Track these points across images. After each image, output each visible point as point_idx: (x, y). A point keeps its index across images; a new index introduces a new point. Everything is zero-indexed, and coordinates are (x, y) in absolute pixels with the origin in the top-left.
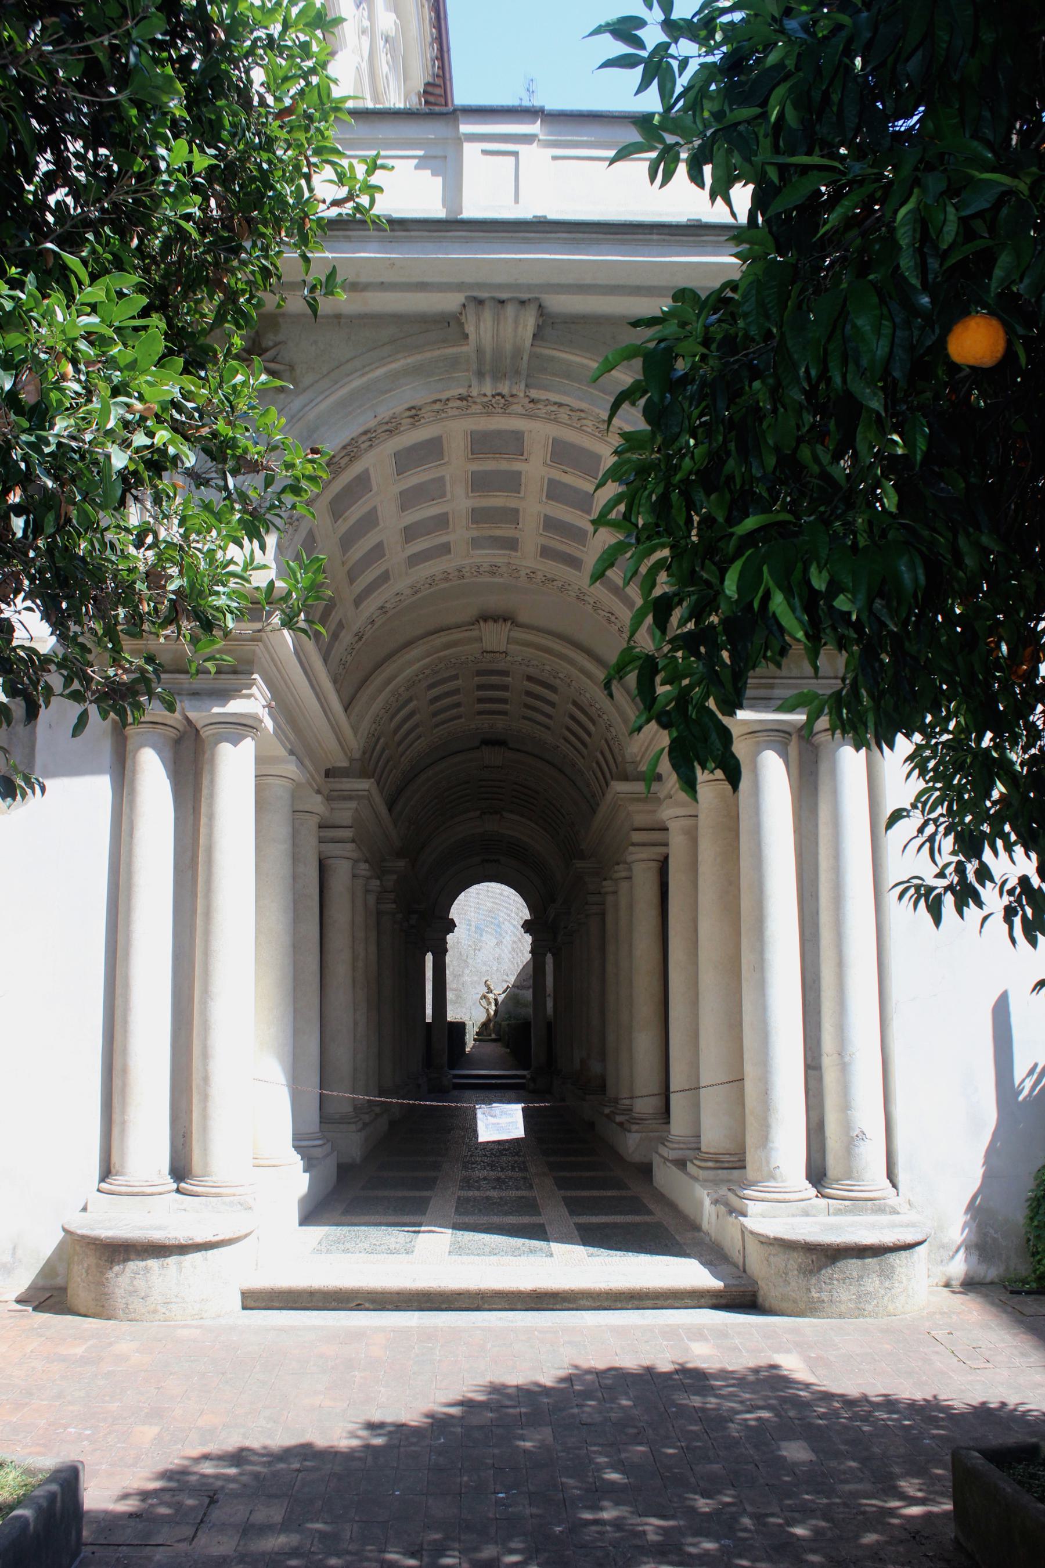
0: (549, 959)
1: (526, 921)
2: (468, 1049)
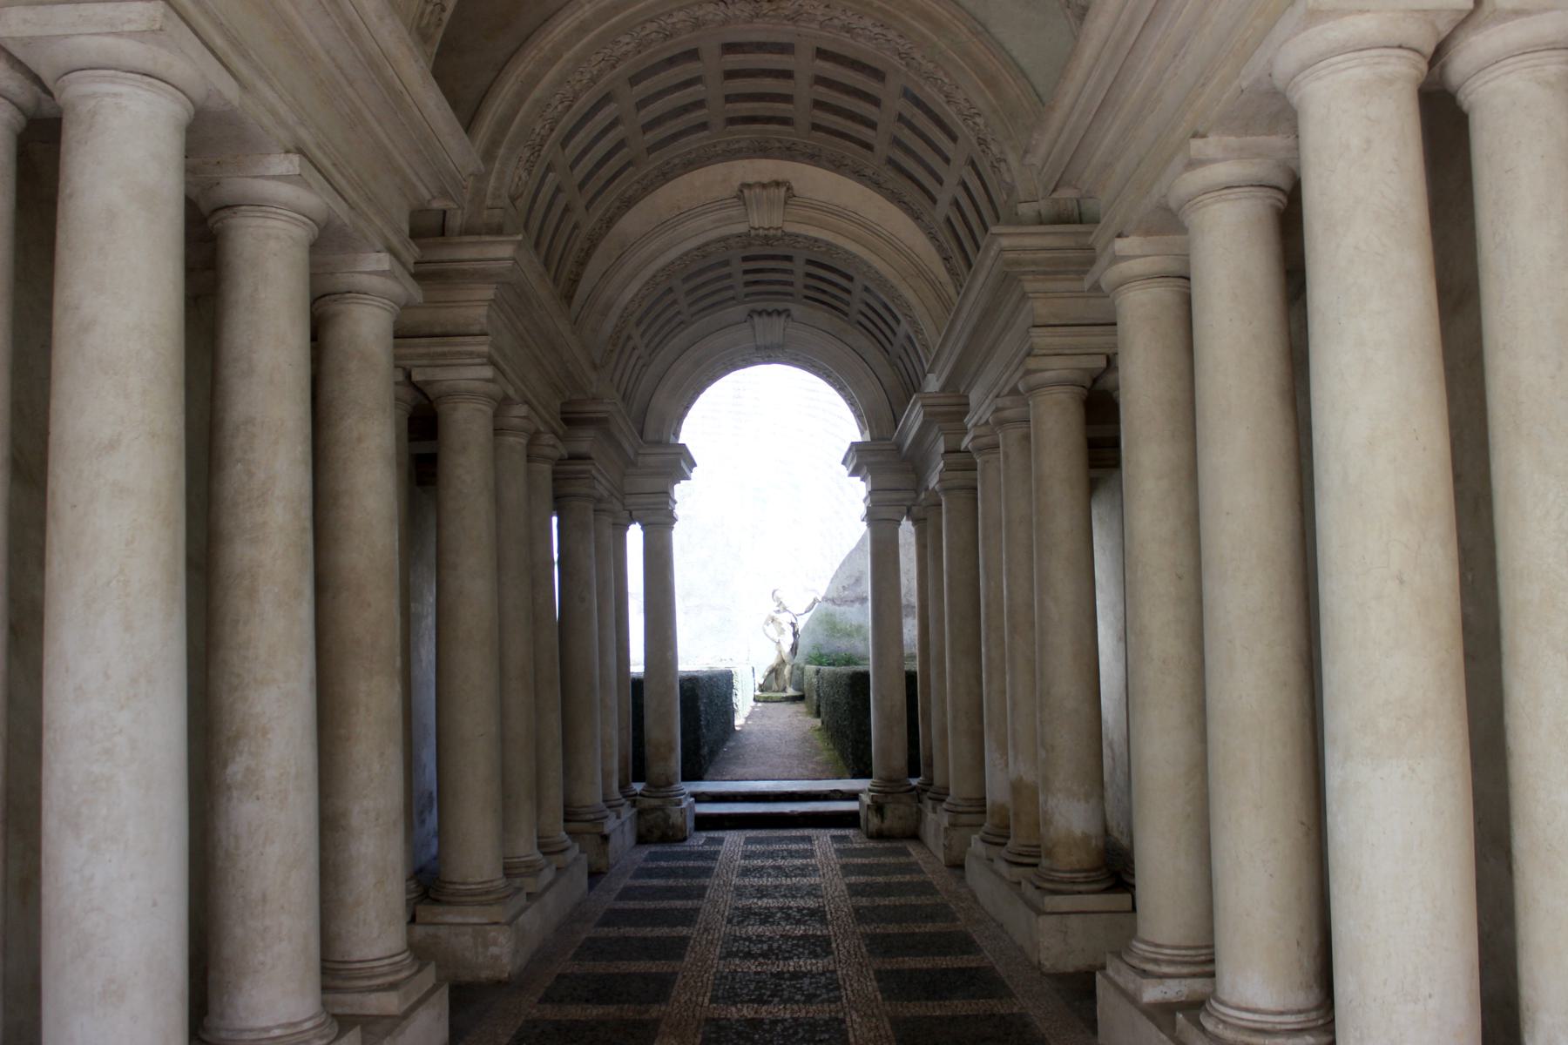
0: (907, 532)
2: (739, 721)
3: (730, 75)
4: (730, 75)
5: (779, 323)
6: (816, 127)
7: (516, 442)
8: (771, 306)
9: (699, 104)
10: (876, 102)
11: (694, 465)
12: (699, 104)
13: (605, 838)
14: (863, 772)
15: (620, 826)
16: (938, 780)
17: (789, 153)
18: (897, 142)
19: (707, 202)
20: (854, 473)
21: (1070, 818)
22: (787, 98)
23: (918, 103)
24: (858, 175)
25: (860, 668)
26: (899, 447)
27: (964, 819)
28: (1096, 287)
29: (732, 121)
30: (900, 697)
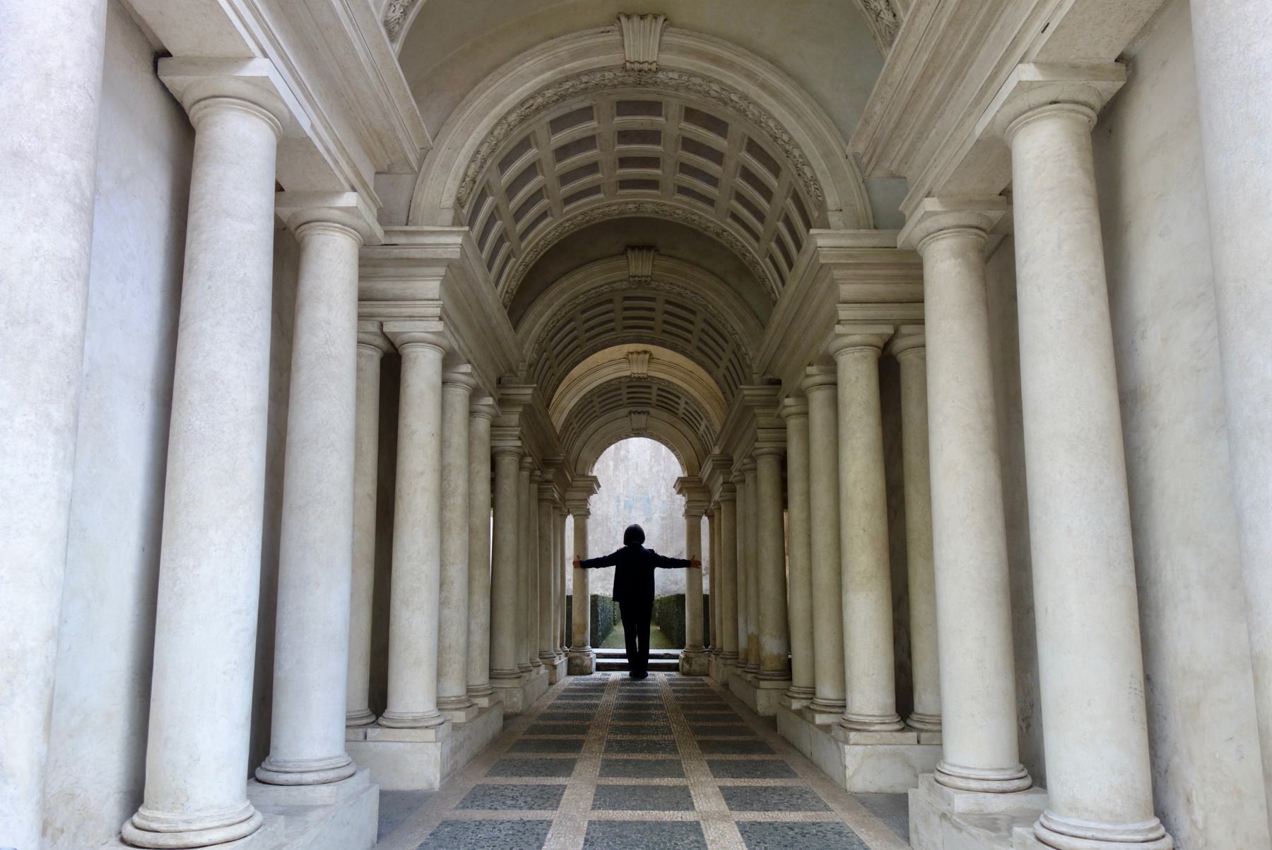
0: (705, 521)
1: (680, 480)
3: (626, 309)
4: (626, 309)
5: (644, 417)
6: (664, 331)
7: (525, 473)
8: (640, 409)
9: (611, 321)
10: (692, 323)
11: (599, 486)
12: (611, 321)
13: (555, 667)
14: (681, 646)
15: (561, 662)
16: (718, 645)
17: (652, 342)
18: (701, 340)
19: (609, 364)
20: (679, 493)
21: (771, 646)
22: (652, 319)
23: (710, 325)
24: (684, 353)
25: (681, 592)
26: (701, 480)
27: (729, 662)
28: (779, 416)
29: (625, 328)
30: (700, 604)
